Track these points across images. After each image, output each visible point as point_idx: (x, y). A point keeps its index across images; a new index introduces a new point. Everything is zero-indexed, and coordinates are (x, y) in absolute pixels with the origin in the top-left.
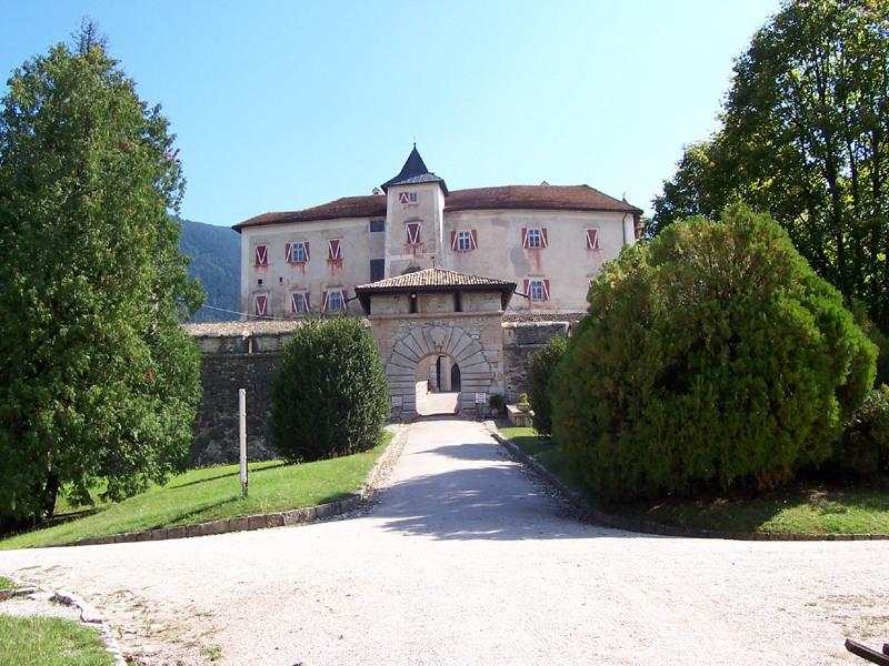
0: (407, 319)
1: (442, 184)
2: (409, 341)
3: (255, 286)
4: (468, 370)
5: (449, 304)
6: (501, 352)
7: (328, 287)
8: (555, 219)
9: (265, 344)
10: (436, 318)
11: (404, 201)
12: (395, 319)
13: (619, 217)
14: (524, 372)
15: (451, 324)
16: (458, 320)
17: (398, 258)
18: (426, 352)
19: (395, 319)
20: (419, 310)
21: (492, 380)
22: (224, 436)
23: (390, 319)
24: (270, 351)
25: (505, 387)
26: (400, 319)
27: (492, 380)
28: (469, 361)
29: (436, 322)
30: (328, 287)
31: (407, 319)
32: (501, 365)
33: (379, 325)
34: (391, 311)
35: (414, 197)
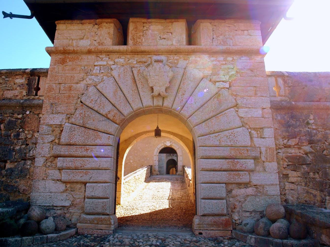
12: (89, 52)
14: (307, 148)
18: (136, 105)
19: (89, 52)
23: (82, 53)
26: (98, 53)
31: (109, 53)
32: (269, 133)
33: (63, 62)
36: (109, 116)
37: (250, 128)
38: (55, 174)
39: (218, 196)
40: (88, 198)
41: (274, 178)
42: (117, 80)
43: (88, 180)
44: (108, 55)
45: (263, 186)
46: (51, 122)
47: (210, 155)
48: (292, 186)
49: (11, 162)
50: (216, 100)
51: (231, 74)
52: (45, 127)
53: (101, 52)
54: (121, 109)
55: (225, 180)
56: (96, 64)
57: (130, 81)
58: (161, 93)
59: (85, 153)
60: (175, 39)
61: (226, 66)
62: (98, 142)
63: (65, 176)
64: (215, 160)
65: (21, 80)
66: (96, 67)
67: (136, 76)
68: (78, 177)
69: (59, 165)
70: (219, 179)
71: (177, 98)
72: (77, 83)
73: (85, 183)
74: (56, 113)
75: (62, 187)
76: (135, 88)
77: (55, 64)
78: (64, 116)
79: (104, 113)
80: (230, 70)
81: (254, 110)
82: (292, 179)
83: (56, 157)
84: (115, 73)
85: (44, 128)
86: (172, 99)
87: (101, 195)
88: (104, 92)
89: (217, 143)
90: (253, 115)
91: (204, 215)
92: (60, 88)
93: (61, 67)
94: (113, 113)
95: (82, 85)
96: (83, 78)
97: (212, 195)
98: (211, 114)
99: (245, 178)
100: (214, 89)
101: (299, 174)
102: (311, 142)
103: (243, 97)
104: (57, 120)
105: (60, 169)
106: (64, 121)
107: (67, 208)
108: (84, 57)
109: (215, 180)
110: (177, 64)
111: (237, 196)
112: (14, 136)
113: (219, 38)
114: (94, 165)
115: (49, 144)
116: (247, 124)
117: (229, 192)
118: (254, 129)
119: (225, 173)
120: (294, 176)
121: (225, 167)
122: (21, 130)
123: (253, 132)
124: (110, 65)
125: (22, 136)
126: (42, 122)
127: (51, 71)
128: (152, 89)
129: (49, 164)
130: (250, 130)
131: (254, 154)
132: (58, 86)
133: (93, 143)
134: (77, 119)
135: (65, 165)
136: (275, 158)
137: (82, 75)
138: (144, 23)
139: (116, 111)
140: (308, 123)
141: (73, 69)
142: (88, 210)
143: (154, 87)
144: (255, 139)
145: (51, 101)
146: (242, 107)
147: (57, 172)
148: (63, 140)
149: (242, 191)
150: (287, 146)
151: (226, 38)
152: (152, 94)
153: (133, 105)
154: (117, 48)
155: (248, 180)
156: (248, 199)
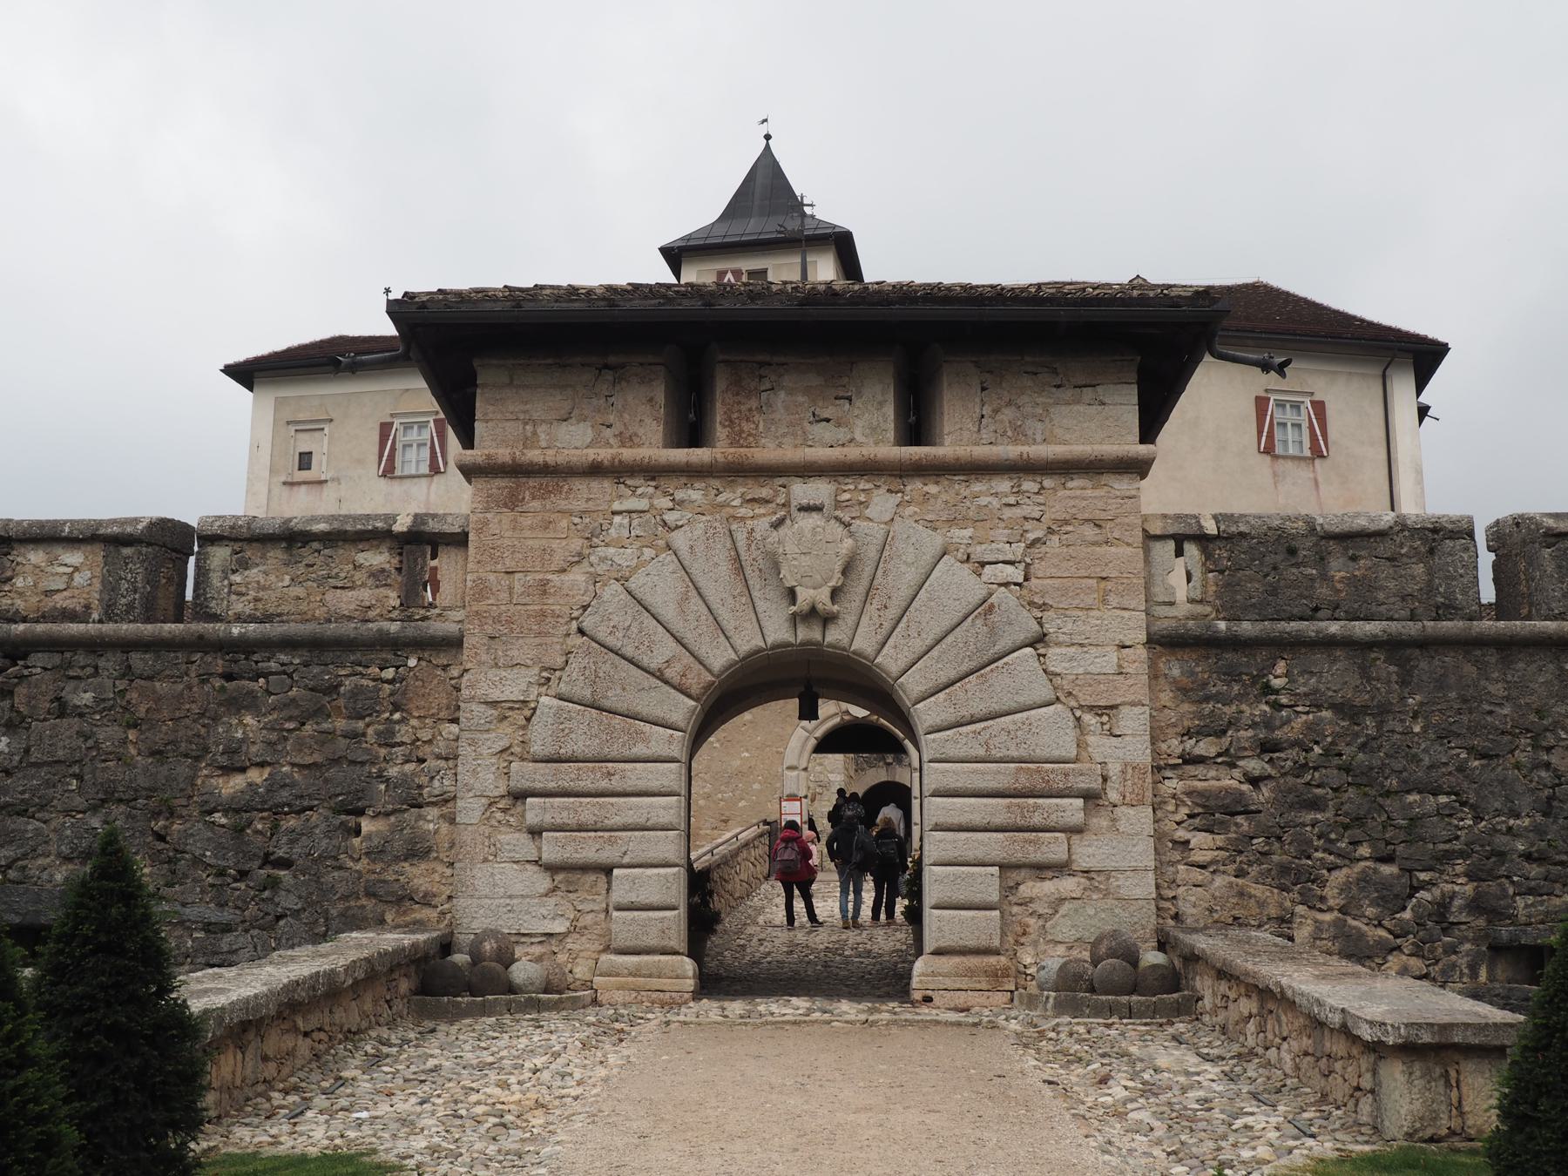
0: (653, 472)
4: (963, 742)
6: (1142, 653)
12: (595, 470)
14: (1254, 765)
21: (1090, 797)
25: (1159, 837)
27: (1090, 797)
28: (973, 698)
29: (803, 491)
31: (653, 472)
32: (1134, 721)
33: (512, 502)
36: (669, 673)
37: (1081, 707)
38: (524, 846)
39: (978, 898)
40: (618, 909)
41: (1143, 853)
42: (686, 563)
43: (617, 860)
44: (653, 479)
45: (1106, 873)
46: (495, 695)
47: (959, 785)
48: (1198, 875)
49: (376, 815)
50: (979, 622)
51: (1031, 536)
54: (702, 652)
55: (998, 854)
56: (616, 506)
57: (725, 569)
58: (820, 607)
59: (604, 784)
60: (860, 423)
61: (1018, 512)
62: (640, 750)
63: (553, 848)
64: (973, 800)
65: (378, 558)
66: (617, 519)
68: (589, 850)
69: (532, 818)
70: (979, 854)
71: (865, 619)
72: (564, 571)
73: (607, 870)
74: (506, 667)
75: (543, 882)
76: (740, 588)
77: (487, 510)
79: (653, 666)
80: (1028, 526)
81: (1093, 650)
82: (1198, 857)
83: (519, 796)
84: (680, 540)
85: (474, 713)
86: (850, 620)
87: (655, 899)
88: (649, 599)
89: (981, 752)
90: (1092, 669)
91: (938, 952)
92: (511, 589)
93: (507, 516)
96: (579, 554)
97: (961, 896)
98: (965, 668)
99: (1053, 848)
100: (974, 589)
101: (1220, 840)
102: (1267, 748)
103: (1063, 612)
104: (513, 686)
105: (535, 832)
107: (561, 936)
108: (580, 485)
109: (970, 855)
111: (1031, 900)
112: (378, 734)
113: (999, 417)
114: (630, 818)
115: (493, 760)
116: (1070, 694)
117: (1009, 889)
118: (1091, 708)
119: (1000, 835)
120: (1203, 844)
121: (999, 820)
122: (397, 716)
123: (1089, 718)
125: (403, 734)
126: (465, 693)
127: (479, 531)
128: (791, 594)
129: (499, 815)
130: (1078, 713)
131: (1083, 784)
132: (505, 580)
133: (627, 753)
134: (574, 681)
135: (548, 819)
136: (1149, 794)
137: (577, 544)
138: (762, 364)
139: (687, 659)
140: (1268, 690)
141: (547, 525)
142: (623, 938)
143: (798, 589)
144: (1091, 739)
145: (489, 630)
146: (1058, 644)
147: (524, 838)
149: (1049, 887)
150: (1190, 760)
151: (1025, 417)
152: (793, 609)
153: (737, 641)
154: (681, 455)
155: (1065, 857)
156: (1064, 909)
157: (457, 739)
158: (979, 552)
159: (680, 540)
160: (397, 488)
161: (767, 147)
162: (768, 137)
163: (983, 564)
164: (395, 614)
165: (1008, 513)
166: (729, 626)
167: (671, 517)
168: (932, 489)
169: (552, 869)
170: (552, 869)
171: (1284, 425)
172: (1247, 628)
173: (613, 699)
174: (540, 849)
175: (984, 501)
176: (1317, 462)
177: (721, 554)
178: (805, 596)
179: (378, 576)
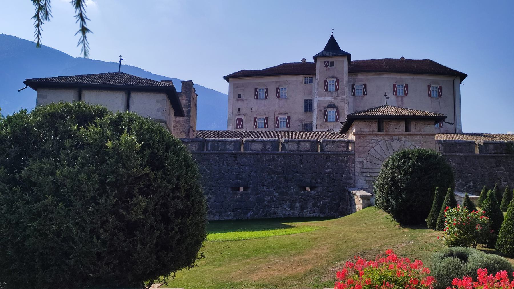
0: (376, 135)
1: (349, 56)
2: (378, 148)
3: (236, 112)
5: (402, 126)
7: (279, 114)
8: (413, 79)
9: (290, 146)
10: (395, 135)
11: (326, 66)
12: (370, 134)
13: (451, 79)
15: (404, 139)
16: (408, 136)
17: (321, 99)
19: (370, 134)
20: (384, 130)
22: (265, 201)
23: (367, 135)
24: (293, 151)
26: (372, 135)
30: (279, 114)
34: (367, 130)
35: (332, 64)
36: (379, 159)
38: (363, 178)
46: (359, 161)
51: (421, 143)
52: (357, 162)
53: (374, 135)
56: (372, 139)
57: (385, 147)
59: (372, 171)
61: (420, 140)
62: (376, 168)
63: (366, 179)
65: (343, 144)
66: (372, 140)
67: (387, 144)
75: (365, 182)
78: (363, 159)
79: (377, 158)
83: (363, 172)
84: (380, 143)
85: (356, 163)
94: (380, 158)
95: (368, 148)
104: (361, 160)
105: (365, 177)
106: (364, 160)
108: (367, 136)
110: (402, 139)
124: (377, 139)
128: (394, 150)
132: (359, 148)
133: (375, 168)
140: (449, 161)
141: (364, 141)
148: (364, 167)
154: (379, 133)
157: (354, 166)
158: (415, 145)
159: (380, 143)
160: (259, 102)
161: (332, 34)
162: (332, 33)
163: (416, 146)
164: (346, 151)
165: (419, 140)
166: (386, 153)
167: (378, 140)
168: (410, 137)
169: (367, 181)
170: (367, 181)
171: (434, 91)
172: (447, 154)
173: (373, 161)
174: (365, 179)
175: (416, 138)
176: (440, 98)
177: (385, 145)
178: (395, 150)
179: (343, 146)
